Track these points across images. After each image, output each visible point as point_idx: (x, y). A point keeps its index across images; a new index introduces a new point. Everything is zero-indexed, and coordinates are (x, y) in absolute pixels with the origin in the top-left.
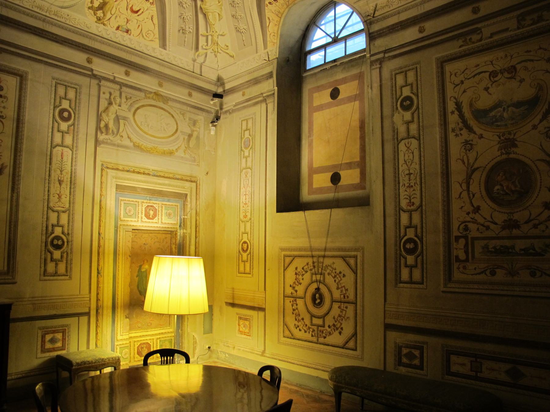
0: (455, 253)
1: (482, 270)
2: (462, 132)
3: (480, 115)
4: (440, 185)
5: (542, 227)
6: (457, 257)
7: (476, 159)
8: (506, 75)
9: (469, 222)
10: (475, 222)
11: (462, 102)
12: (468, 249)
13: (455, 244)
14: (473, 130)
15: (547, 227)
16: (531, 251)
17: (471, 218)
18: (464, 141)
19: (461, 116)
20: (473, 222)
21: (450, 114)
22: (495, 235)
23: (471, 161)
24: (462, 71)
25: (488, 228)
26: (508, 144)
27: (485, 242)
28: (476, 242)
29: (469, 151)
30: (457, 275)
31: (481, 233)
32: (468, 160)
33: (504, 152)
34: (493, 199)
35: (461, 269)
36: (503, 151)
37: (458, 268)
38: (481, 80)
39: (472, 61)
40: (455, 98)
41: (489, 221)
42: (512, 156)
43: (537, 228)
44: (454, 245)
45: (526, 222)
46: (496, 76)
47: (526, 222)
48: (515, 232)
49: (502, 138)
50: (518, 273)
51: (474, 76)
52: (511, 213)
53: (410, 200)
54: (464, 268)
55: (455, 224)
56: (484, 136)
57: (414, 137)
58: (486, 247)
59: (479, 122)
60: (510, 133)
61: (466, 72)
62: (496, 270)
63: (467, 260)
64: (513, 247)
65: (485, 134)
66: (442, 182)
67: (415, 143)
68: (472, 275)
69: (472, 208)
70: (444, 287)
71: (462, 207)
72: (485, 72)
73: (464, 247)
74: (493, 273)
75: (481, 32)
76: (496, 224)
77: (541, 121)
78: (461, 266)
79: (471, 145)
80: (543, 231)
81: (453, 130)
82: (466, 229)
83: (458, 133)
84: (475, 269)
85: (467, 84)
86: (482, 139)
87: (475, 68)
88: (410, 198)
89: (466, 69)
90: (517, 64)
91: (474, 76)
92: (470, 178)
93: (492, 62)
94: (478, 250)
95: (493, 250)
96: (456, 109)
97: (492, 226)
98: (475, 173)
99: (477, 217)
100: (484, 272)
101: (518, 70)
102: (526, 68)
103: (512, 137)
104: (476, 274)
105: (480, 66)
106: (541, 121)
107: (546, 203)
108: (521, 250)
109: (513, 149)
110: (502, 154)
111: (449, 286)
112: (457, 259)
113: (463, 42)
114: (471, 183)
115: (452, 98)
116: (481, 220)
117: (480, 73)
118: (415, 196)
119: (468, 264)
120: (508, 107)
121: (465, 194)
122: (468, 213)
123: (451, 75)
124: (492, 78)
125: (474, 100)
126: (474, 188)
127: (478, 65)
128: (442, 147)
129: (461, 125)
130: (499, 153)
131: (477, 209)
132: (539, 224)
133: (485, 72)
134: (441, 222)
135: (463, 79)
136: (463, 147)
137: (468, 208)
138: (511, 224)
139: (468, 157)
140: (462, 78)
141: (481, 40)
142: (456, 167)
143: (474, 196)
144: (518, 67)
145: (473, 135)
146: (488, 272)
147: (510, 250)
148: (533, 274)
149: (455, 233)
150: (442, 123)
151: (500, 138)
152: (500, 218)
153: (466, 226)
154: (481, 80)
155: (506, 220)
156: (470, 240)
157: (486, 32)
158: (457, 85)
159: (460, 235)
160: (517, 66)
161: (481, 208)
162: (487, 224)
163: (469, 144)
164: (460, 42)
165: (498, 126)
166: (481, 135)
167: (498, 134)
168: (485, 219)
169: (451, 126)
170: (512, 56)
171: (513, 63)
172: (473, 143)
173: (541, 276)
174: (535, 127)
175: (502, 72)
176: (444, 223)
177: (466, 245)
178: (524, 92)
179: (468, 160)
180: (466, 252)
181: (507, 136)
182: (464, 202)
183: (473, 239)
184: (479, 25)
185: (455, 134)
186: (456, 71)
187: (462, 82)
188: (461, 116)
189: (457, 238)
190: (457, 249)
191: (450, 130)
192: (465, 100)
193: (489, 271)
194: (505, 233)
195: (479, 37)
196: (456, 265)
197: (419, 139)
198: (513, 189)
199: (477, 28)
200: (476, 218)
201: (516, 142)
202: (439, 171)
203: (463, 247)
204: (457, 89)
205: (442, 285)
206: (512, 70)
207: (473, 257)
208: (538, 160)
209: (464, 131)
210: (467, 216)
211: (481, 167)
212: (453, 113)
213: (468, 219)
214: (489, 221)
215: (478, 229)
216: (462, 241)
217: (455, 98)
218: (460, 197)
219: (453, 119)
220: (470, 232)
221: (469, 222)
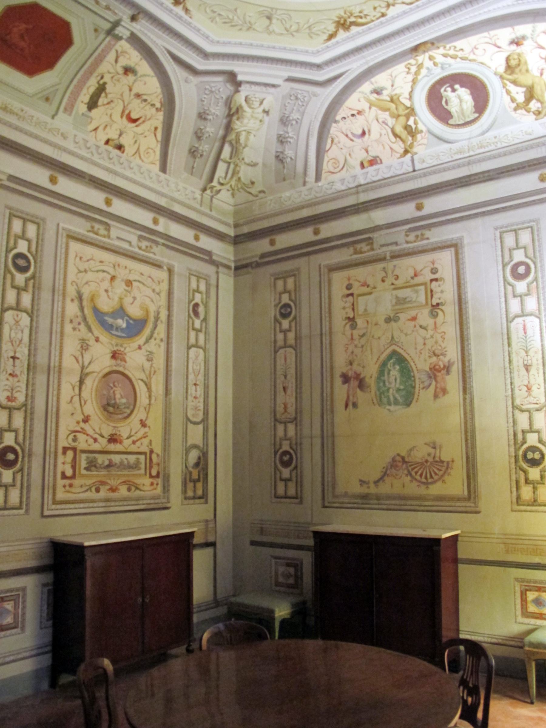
1: (87, 487)
5: (138, 444)
6: (63, 474)
7: (90, 363)
15: (142, 444)
17: (82, 428)
19: (82, 309)
24: (88, 258)
25: (95, 440)
35: (67, 488)
37: (64, 486)
38: (103, 280)
40: (77, 285)
44: (61, 458)
45: (128, 438)
47: (128, 438)
51: (98, 271)
53: (12, 394)
56: (100, 339)
57: (25, 311)
61: (91, 262)
65: (102, 338)
67: (25, 320)
72: (108, 273)
74: (98, 490)
76: (103, 437)
77: (144, 344)
79: (88, 345)
82: (75, 440)
83: (77, 326)
84: (81, 486)
85: (90, 276)
87: (98, 264)
88: (12, 390)
89: (92, 259)
90: (135, 281)
91: (98, 271)
93: (114, 266)
97: (100, 439)
99: (86, 427)
100: (90, 489)
103: (122, 349)
104: (83, 492)
105: (104, 264)
106: (144, 344)
112: (64, 476)
116: (91, 432)
117: (104, 271)
118: (18, 389)
121: (76, 398)
122: (78, 423)
123: (76, 256)
126: (85, 394)
129: (80, 319)
132: (137, 441)
133: (108, 273)
135: (88, 269)
140: (86, 266)
143: (85, 403)
145: (90, 334)
146: (93, 489)
148: (129, 490)
149: (63, 443)
152: (107, 431)
154: (103, 280)
157: (114, 233)
158: (80, 272)
159: (68, 445)
160: (133, 283)
162: (96, 436)
164: (88, 225)
168: (94, 430)
171: (131, 278)
172: (90, 343)
174: (140, 348)
180: (74, 467)
186: (82, 255)
187: (86, 271)
188: (82, 309)
192: (86, 292)
197: (31, 317)
209: (82, 327)
211: (93, 372)
213: (78, 429)
215: (87, 441)
216: (70, 454)
217: (77, 285)
218: (71, 401)
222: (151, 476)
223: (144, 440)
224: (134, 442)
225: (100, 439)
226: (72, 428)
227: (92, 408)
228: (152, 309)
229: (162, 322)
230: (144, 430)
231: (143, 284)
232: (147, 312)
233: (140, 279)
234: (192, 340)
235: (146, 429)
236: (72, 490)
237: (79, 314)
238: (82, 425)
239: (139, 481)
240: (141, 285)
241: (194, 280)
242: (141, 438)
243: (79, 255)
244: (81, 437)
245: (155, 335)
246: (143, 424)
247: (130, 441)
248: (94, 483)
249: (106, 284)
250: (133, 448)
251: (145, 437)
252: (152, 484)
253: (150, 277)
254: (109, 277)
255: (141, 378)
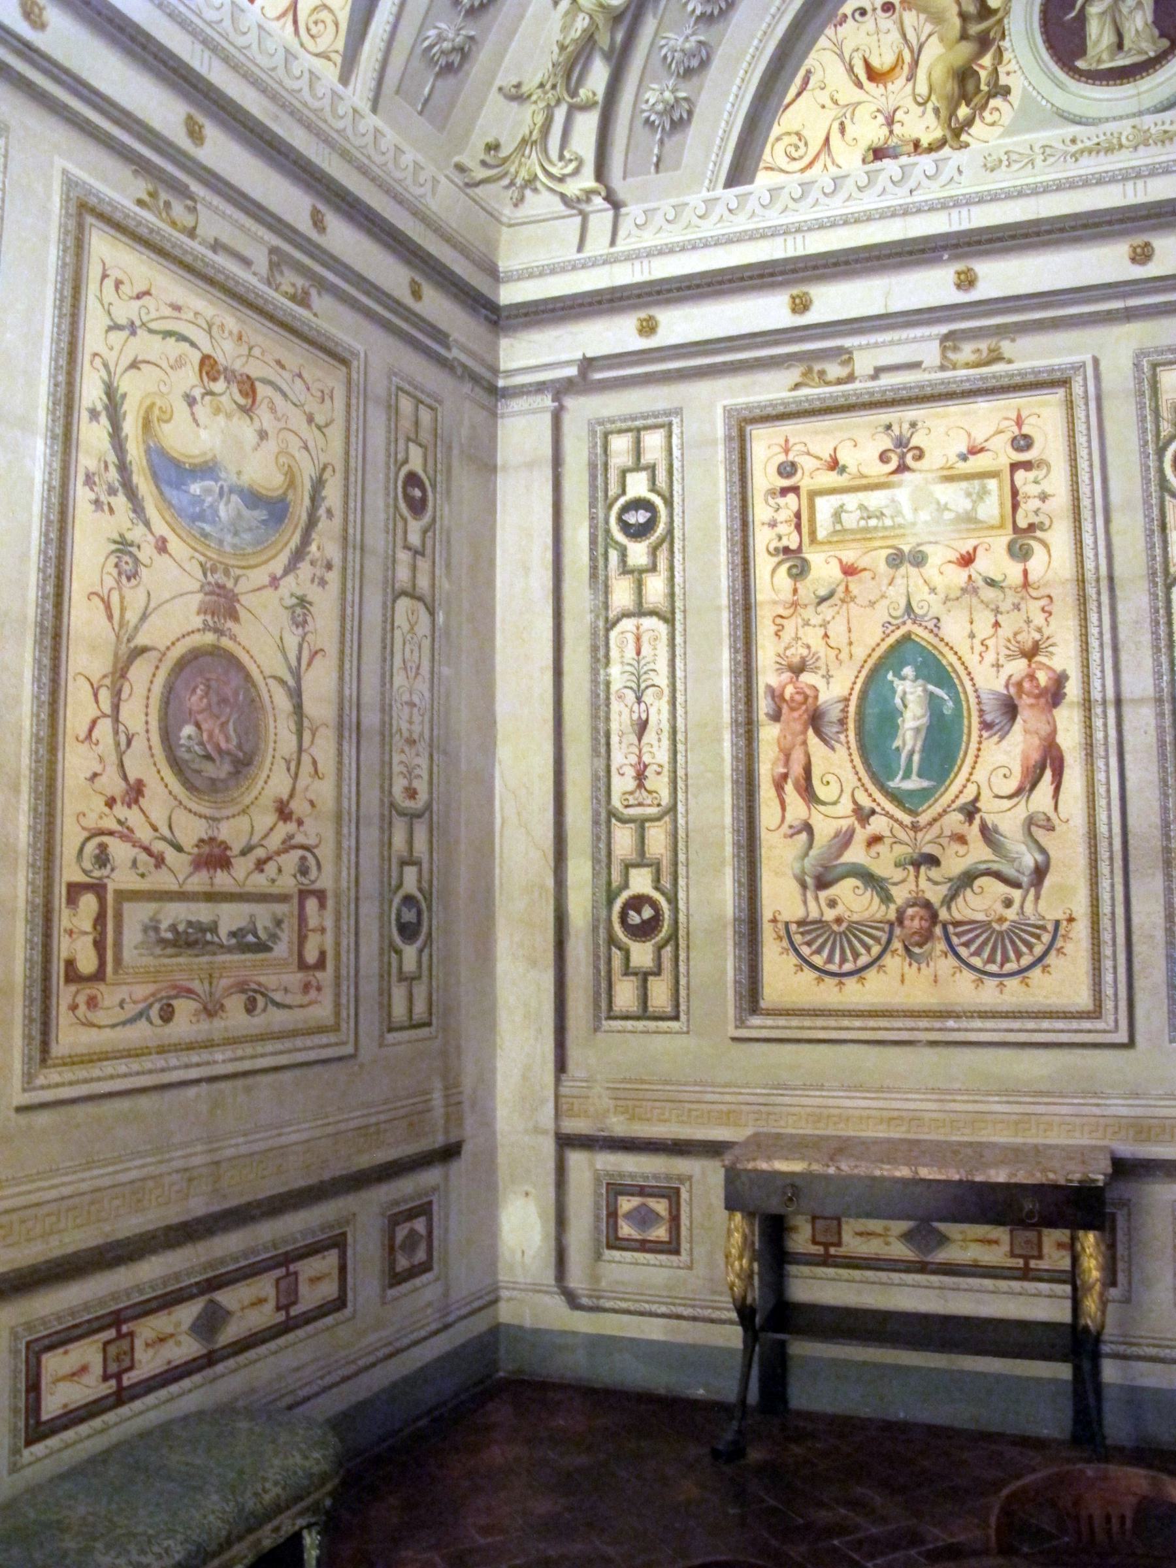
0: (64, 948)
1: (141, 1006)
2: (112, 500)
3: (172, 471)
4: (28, 674)
6: (70, 963)
7: (144, 617)
8: (235, 389)
9: (111, 833)
10: (126, 834)
11: (124, 396)
12: (103, 934)
13: (66, 912)
14: (143, 509)
15: (280, 870)
16: (251, 938)
17: (119, 822)
18: (118, 539)
20: (122, 837)
21: (85, 415)
22: (175, 887)
23: (132, 617)
25: (160, 861)
26: (222, 604)
27: (153, 906)
28: (127, 907)
29: (129, 579)
30: (69, 1037)
31: (143, 876)
32: (123, 609)
33: (211, 623)
34: (176, 764)
35: (82, 1008)
36: (209, 618)
38: (179, 363)
39: (170, 287)
40: (106, 366)
41: (164, 839)
42: (225, 642)
43: (262, 871)
44: (64, 918)
45: (243, 853)
46: (215, 379)
47: (243, 853)
48: (223, 880)
49: (210, 578)
50: (222, 1006)
51: (168, 334)
52: (214, 819)
54: (92, 1003)
55: (70, 837)
56: (170, 547)
58: (152, 927)
59: (161, 493)
60: (227, 573)
62: (174, 1002)
63: (99, 976)
64: (213, 928)
65: (174, 544)
66: (38, 662)
68: (113, 1026)
69: (123, 784)
70: (24, 1090)
71: (95, 775)
72: (193, 344)
73: (95, 927)
74: (167, 1015)
75: (195, 209)
76: (179, 849)
77: (287, 571)
78: (81, 999)
79: (136, 560)
80: (273, 881)
81: (89, 480)
82: (102, 858)
83: (104, 498)
84: (121, 1005)
85: (147, 346)
86: (165, 556)
87: (168, 312)
92: (123, 676)
93: (210, 327)
94: (132, 935)
95: (169, 935)
96: (106, 408)
97: (170, 855)
98: (138, 663)
99: (133, 816)
101: (259, 398)
102: (273, 410)
103: (230, 584)
104: (124, 1023)
106: (287, 571)
107: (281, 801)
108: (233, 934)
109: (230, 624)
110: (206, 628)
111: (40, 1081)
112: (72, 975)
113: (151, 195)
114: (124, 696)
115: (98, 360)
116: (144, 834)
117: (184, 339)
119: (102, 987)
120: (231, 491)
121: (105, 728)
123: (105, 276)
124: (205, 378)
125: (156, 412)
127: (178, 308)
128: (49, 522)
129: (113, 475)
130: (197, 621)
131: (135, 792)
132: (269, 859)
133: (193, 344)
134: (23, 820)
136: (113, 560)
137: (112, 784)
138: (214, 857)
139: (122, 598)
141: (191, 233)
142: (84, 618)
144: (261, 389)
146: (154, 1012)
147: (209, 937)
149: (70, 872)
150: (59, 431)
151: (205, 575)
152: (191, 831)
153: (103, 847)
154: (179, 363)
155: (202, 841)
156: (110, 897)
158: (116, 327)
160: (258, 384)
161: (146, 791)
162: (158, 846)
163: (131, 554)
165: (206, 535)
166: (164, 540)
167: (202, 559)
168: (155, 829)
169: (86, 461)
170: (251, 349)
171: (255, 370)
172: (142, 556)
173: (264, 1010)
174: (274, 582)
175: (230, 376)
176: (32, 828)
177: (100, 919)
178: (260, 470)
179: (123, 609)
180: (99, 945)
181: (219, 577)
182: (101, 759)
183: (124, 896)
184: (195, 187)
185: (93, 496)
186: (121, 276)
187: (132, 329)
189: (75, 891)
190: (71, 933)
191: (81, 478)
193: (157, 1006)
194: (198, 882)
195: (188, 220)
196: (64, 994)
198: (223, 745)
199: (187, 187)
200: (130, 823)
201: (238, 606)
202: (31, 612)
203: (87, 926)
204: (117, 337)
205: (17, 1082)
206: (248, 387)
207: (118, 961)
208: (274, 677)
209: (120, 501)
210: (106, 810)
212: (94, 414)
214: (164, 839)
215: (134, 863)
216: (88, 902)
217: (106, 366)
219: (93, 436)
220: (113, 870)
221: (111, 833)
222: (303, 966)
223: (282, 859)
224: (260, 865)
225: (170, 855)
226: (91, 822)
227: (147, 762)
228: (307, 471)
229: (329, 512)
230: (284, 829)
231: (285, 395)
232: (291, 484)
233: (273, 377)
234: (403, 575)
235: (291, 827)
236: (100, 1017)
237: (112, 458)
238: (120, 811)
239: (269, 980)
240: (278, 399)
241: (406, 405)
242: (278, 853)
243: (114, 274)
244: (120, 851)
245: (313, 548)
246: (283, 812)
247: (250, 861)
248: (153, 995)
249: (188, 378)
250: (259, 882)
251: (286, 851)
252: (306, 987)
253: (300, 376)
254: (196, 357)
255: (279, 674)
